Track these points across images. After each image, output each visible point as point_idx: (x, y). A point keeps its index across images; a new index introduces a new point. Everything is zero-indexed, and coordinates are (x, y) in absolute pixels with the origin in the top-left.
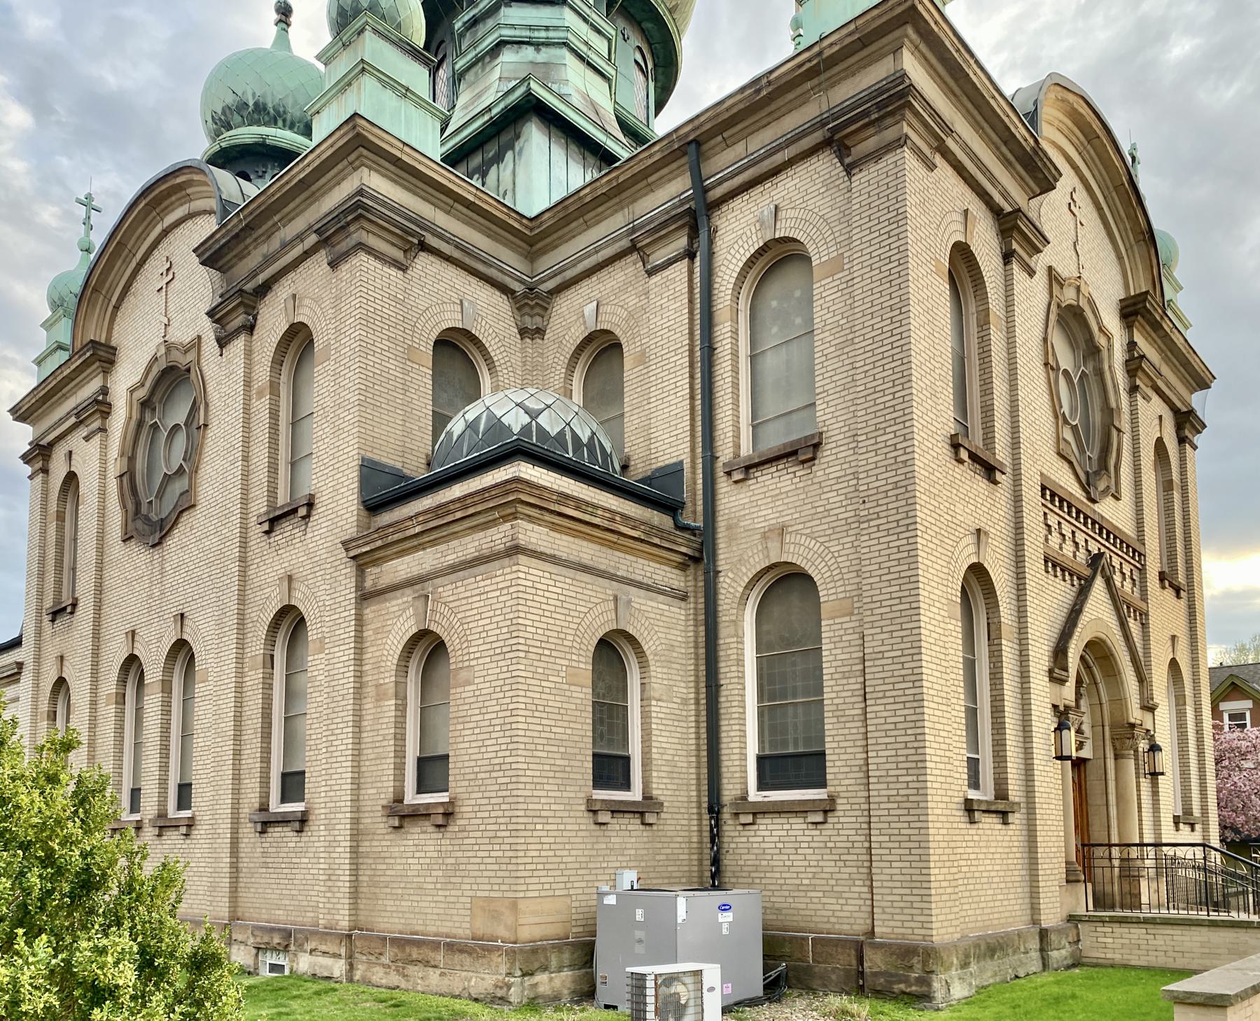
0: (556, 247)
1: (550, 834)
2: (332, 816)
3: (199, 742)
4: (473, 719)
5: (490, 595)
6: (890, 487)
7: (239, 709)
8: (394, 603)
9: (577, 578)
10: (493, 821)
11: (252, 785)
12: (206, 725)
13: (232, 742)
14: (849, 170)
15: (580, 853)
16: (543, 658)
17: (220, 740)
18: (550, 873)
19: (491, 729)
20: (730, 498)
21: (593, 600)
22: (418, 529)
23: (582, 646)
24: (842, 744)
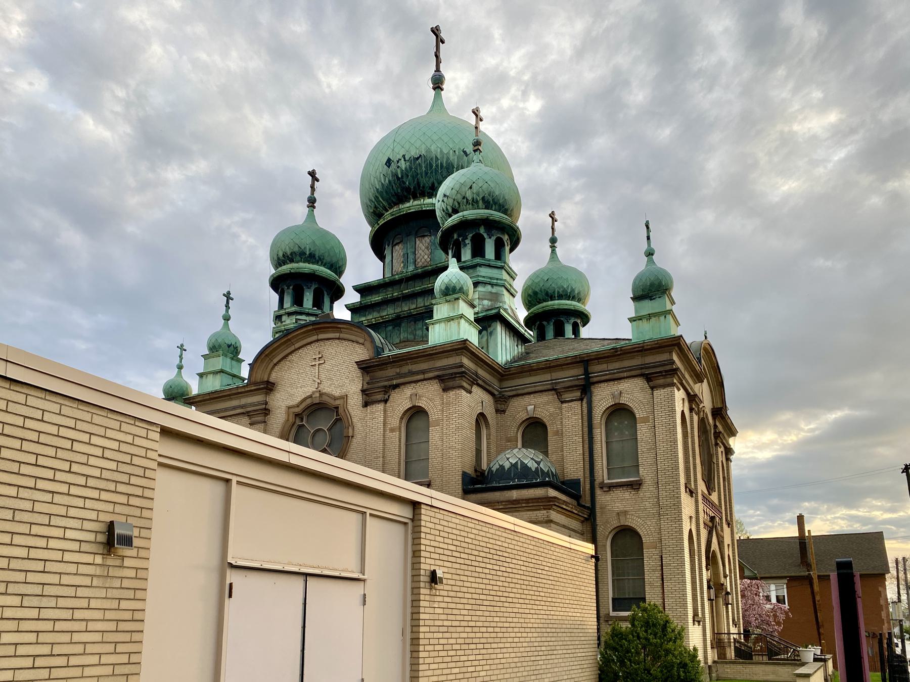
0: (513, 379)
20: (602, 498)
24: (652, 596)
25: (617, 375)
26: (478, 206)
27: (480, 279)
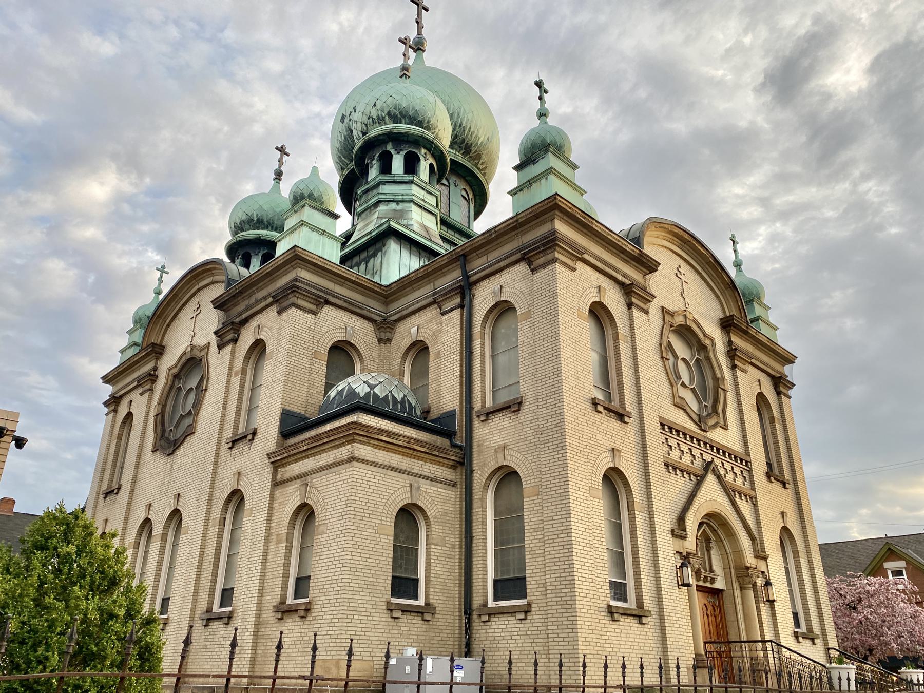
1: (362, 622)
2: (246, 613)
3: (178, 570)
4: (325, 553)
5: (339, 483)
6: (553, 426)
7: (203, 550)
8: (291, 488)
9: (388, 474)
10: (330, 613)
11: (204, 597)
12: (183, 560)
13: (196, 570)
15: (381, 635)
16: (364, 519)
17: (189, 569)
18: (361, 646)
19: (333, 559)
21: (396, 486)
23: (389, 512)
27: (381, 197)
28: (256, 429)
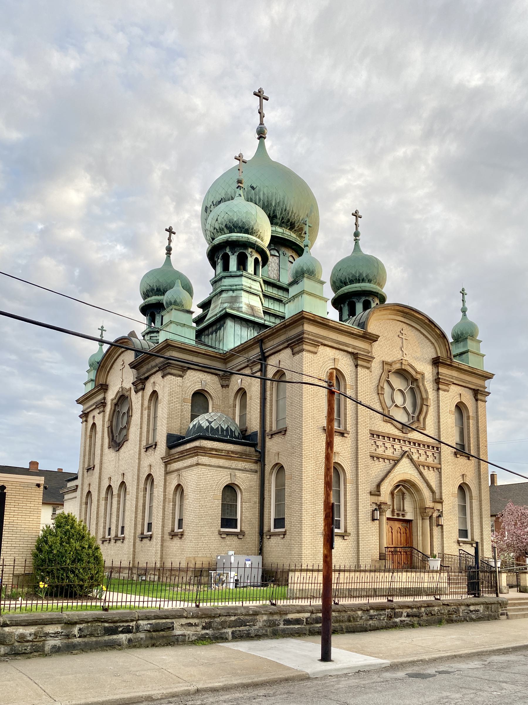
14: (293, 354)
22: (177, 457)
25: (277, 348)
26: (224, 232)
28: (156, 442)
